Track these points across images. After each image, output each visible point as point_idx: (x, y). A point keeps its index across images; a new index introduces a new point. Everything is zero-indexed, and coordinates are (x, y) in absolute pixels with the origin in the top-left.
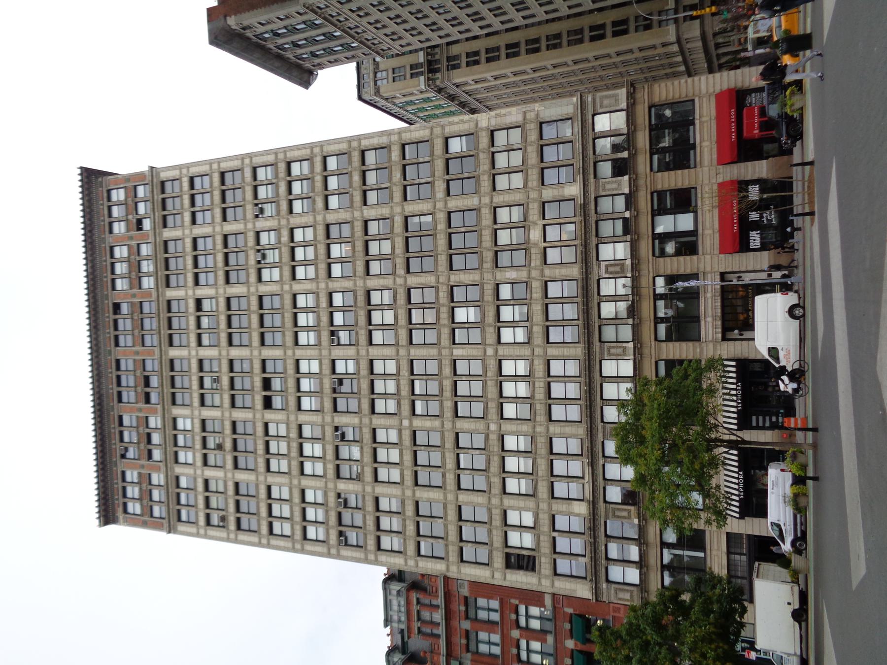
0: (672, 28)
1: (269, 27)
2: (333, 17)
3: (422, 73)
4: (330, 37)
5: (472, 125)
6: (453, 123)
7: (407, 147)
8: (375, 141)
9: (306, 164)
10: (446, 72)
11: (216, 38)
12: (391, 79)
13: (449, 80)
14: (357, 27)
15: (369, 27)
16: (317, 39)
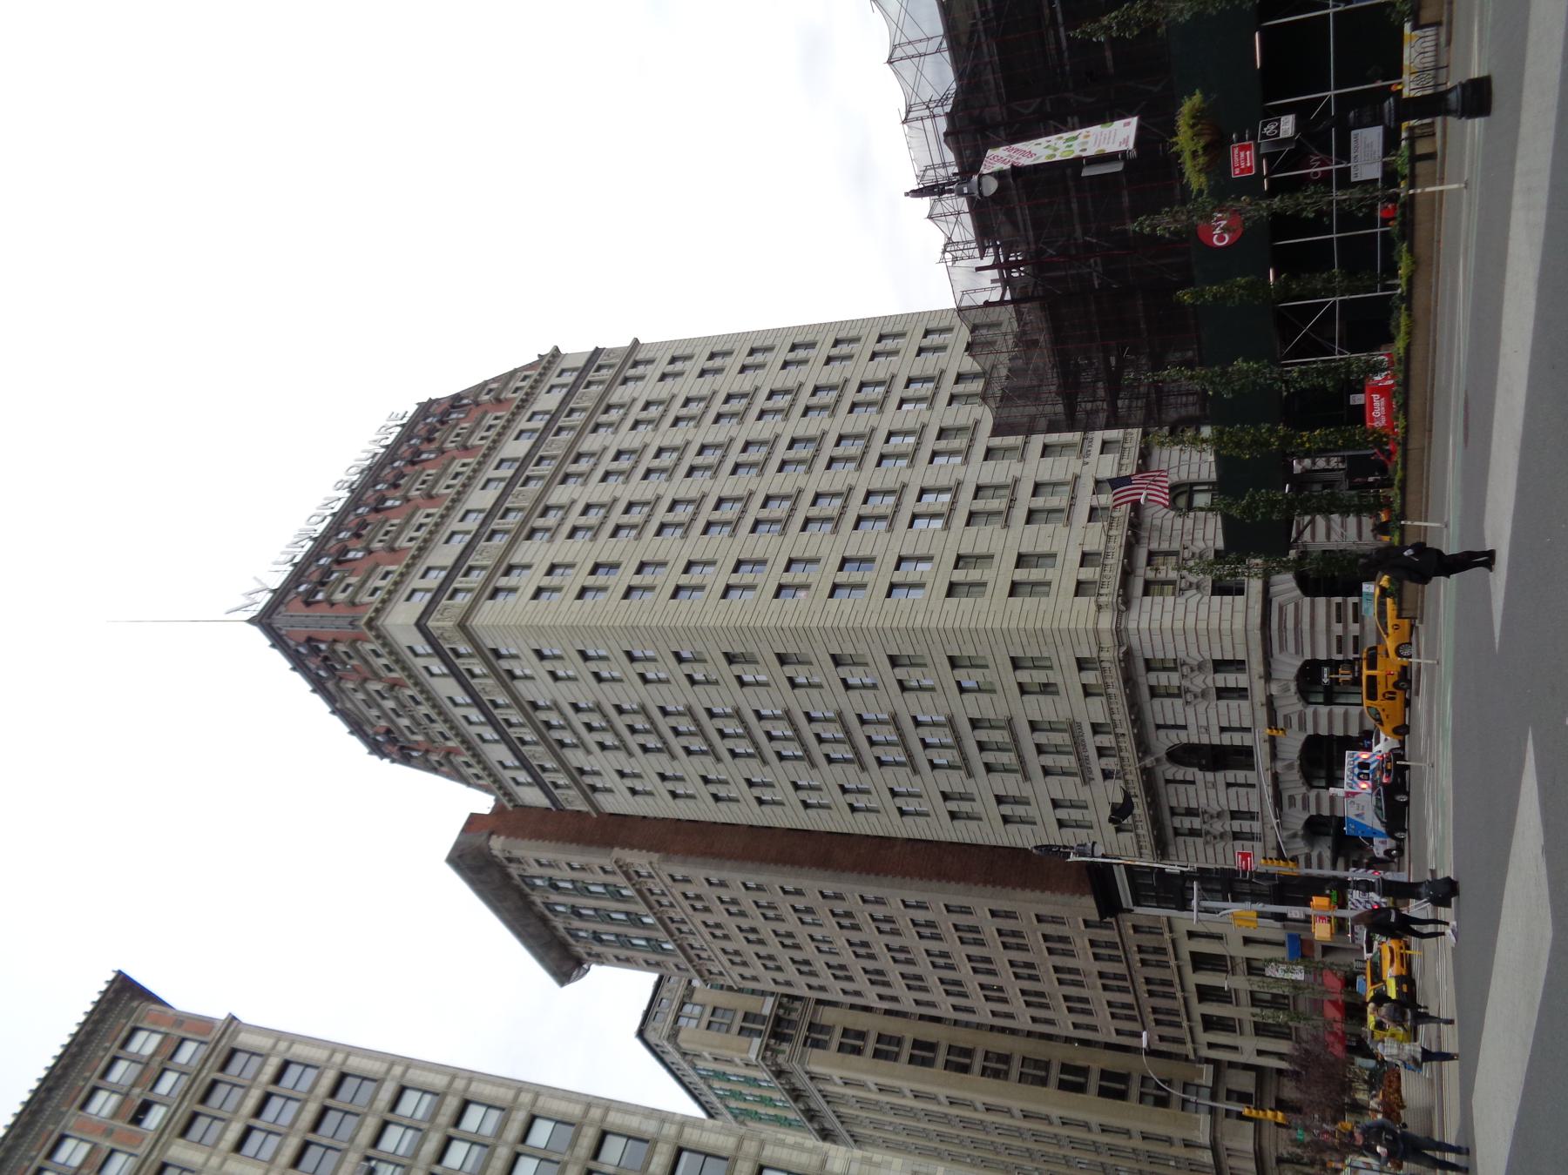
0: (1204, 1120)
1: (549, 872)
2: (652, 893)
3: (759, 1033)
4: (634, 920)
5: (815, 1160)
6: (782, 1144)
7: (685, 1156)
8: (634, 1123)
9: (495, 1115)
10: (800, 1048)
11: (460, 857)
12: (704, 1023)
13: (801, 1061)
14: (683, 922)
15: (703, 928)
16: (614, 916)
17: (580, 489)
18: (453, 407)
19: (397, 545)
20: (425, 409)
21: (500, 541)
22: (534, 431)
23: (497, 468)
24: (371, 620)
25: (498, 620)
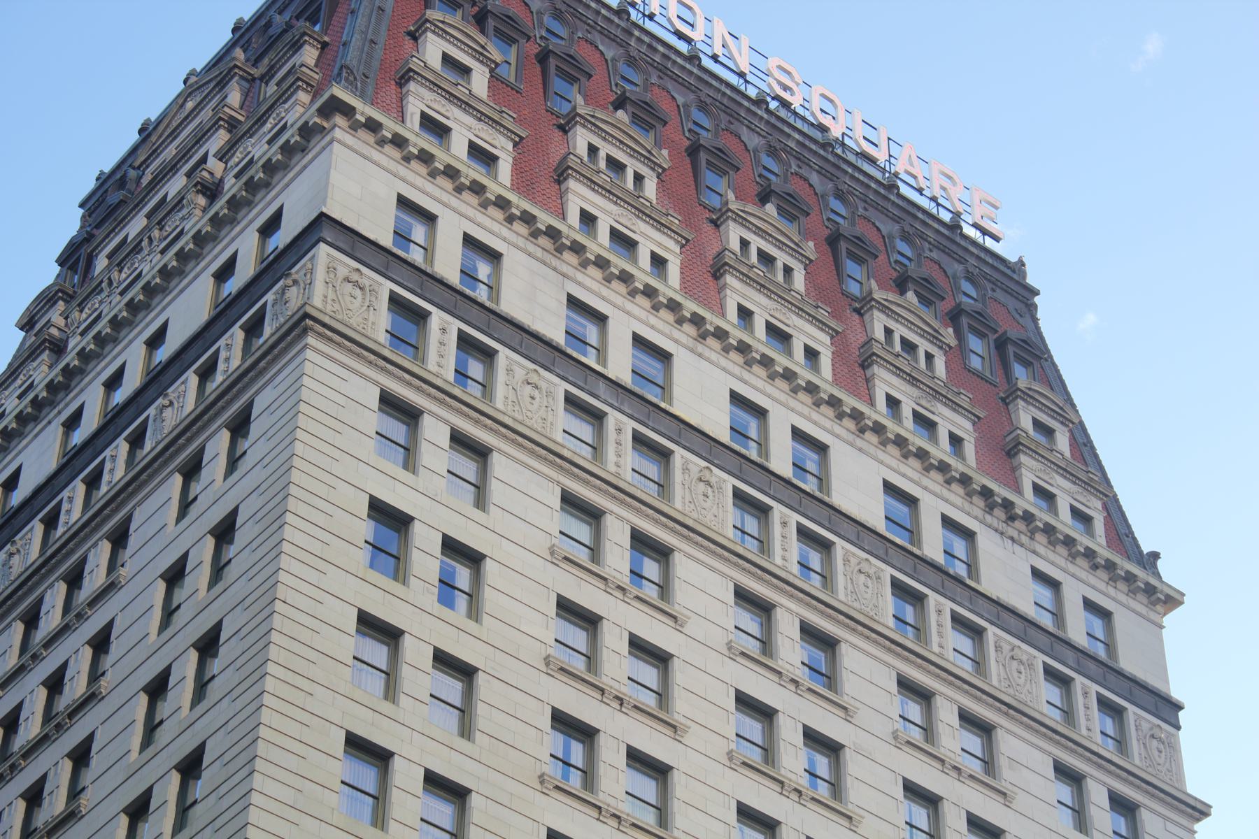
17: (719, 639)
18: (1001, 345)
19: (572, 184)
20: (1010, 282)
21: (561, 426)
22: (913, 533)
23: (948, 522)
24: (348, 111)
25: (329, 411)
